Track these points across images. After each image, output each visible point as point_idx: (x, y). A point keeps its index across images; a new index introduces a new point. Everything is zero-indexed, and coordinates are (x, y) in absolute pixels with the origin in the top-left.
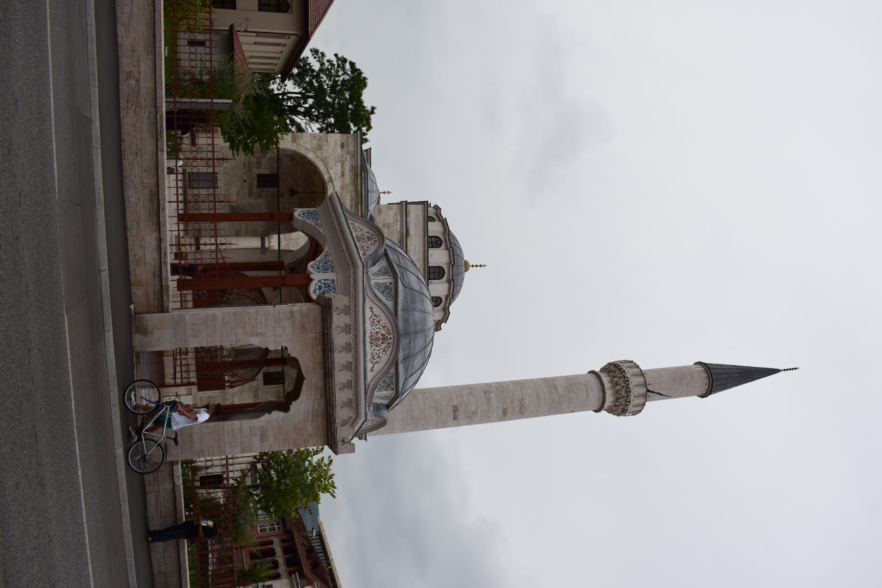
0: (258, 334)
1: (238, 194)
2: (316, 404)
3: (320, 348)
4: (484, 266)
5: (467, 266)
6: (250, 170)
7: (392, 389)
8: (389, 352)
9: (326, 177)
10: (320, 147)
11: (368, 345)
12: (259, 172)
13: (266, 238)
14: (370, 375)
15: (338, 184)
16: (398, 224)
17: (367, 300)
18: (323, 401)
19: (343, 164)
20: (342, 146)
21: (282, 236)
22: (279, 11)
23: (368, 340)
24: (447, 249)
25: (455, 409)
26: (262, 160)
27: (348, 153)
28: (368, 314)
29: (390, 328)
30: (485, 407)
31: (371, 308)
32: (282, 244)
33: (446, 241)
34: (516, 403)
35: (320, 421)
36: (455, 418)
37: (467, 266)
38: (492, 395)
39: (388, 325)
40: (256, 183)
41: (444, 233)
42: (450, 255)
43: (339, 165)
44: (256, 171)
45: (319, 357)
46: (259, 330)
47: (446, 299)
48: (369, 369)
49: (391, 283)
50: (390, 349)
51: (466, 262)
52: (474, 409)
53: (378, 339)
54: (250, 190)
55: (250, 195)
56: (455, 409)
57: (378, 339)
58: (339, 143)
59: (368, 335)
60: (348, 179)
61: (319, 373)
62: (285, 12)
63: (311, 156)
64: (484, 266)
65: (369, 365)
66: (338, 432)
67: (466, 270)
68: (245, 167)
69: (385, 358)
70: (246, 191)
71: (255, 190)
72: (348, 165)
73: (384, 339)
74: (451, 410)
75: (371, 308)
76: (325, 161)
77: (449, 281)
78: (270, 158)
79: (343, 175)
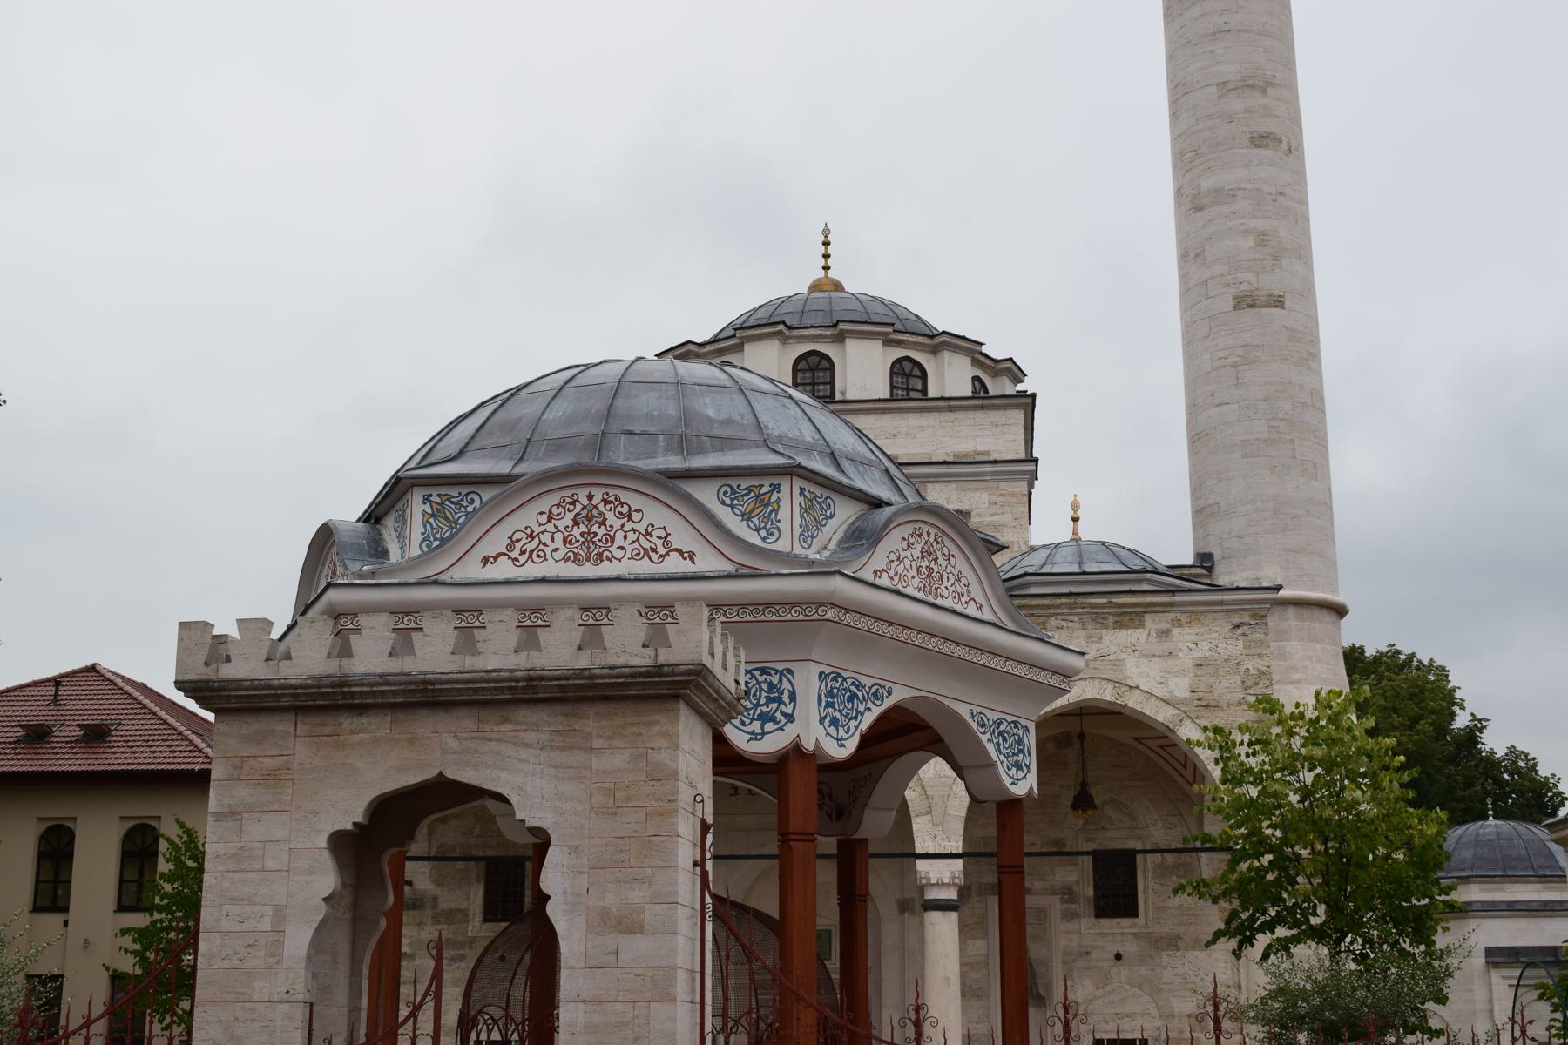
0: (278, 930)
2: (531, 737)
3: (347, 722)
5: (827, 286)
7: (776, 488)
8: (635, 501)
11: (606, 569)
12: (479, 917)
14: (708, 562)
17: (457, 574)
18: (526, 715)
22: (71, 855)
23: (588, 570)
25: (1246, 302)
26: (444, 905)
28: (503, 569)
29: (555, 498)
30: (1243, 205)
31: (486, 560)
34: (1236, 104)
35: (592, 723)
36: (1278, 303)
37: (827, 286)
38: (1207, 183)
39: (546, 504)
42: (760, 338)
45: (376, 726)
46: (266, 925)
47: (899, 344)
48: (687, 567)
49: (427, 499)
50: (625, 496)
51: (815, 287)
52: (1250, 242)
53: (589, 536)
56: (1246, 302)
57: (589, 536)
59: (571, 570)
61: (427, 726)
62: (71, 835)
65: (674, 564)
66: (621, 661)
67: (838, 286)
69: (654, 514)
73: (589, 518)
74: (1248, 317)
75: (486, 560)
77: (840, 338)
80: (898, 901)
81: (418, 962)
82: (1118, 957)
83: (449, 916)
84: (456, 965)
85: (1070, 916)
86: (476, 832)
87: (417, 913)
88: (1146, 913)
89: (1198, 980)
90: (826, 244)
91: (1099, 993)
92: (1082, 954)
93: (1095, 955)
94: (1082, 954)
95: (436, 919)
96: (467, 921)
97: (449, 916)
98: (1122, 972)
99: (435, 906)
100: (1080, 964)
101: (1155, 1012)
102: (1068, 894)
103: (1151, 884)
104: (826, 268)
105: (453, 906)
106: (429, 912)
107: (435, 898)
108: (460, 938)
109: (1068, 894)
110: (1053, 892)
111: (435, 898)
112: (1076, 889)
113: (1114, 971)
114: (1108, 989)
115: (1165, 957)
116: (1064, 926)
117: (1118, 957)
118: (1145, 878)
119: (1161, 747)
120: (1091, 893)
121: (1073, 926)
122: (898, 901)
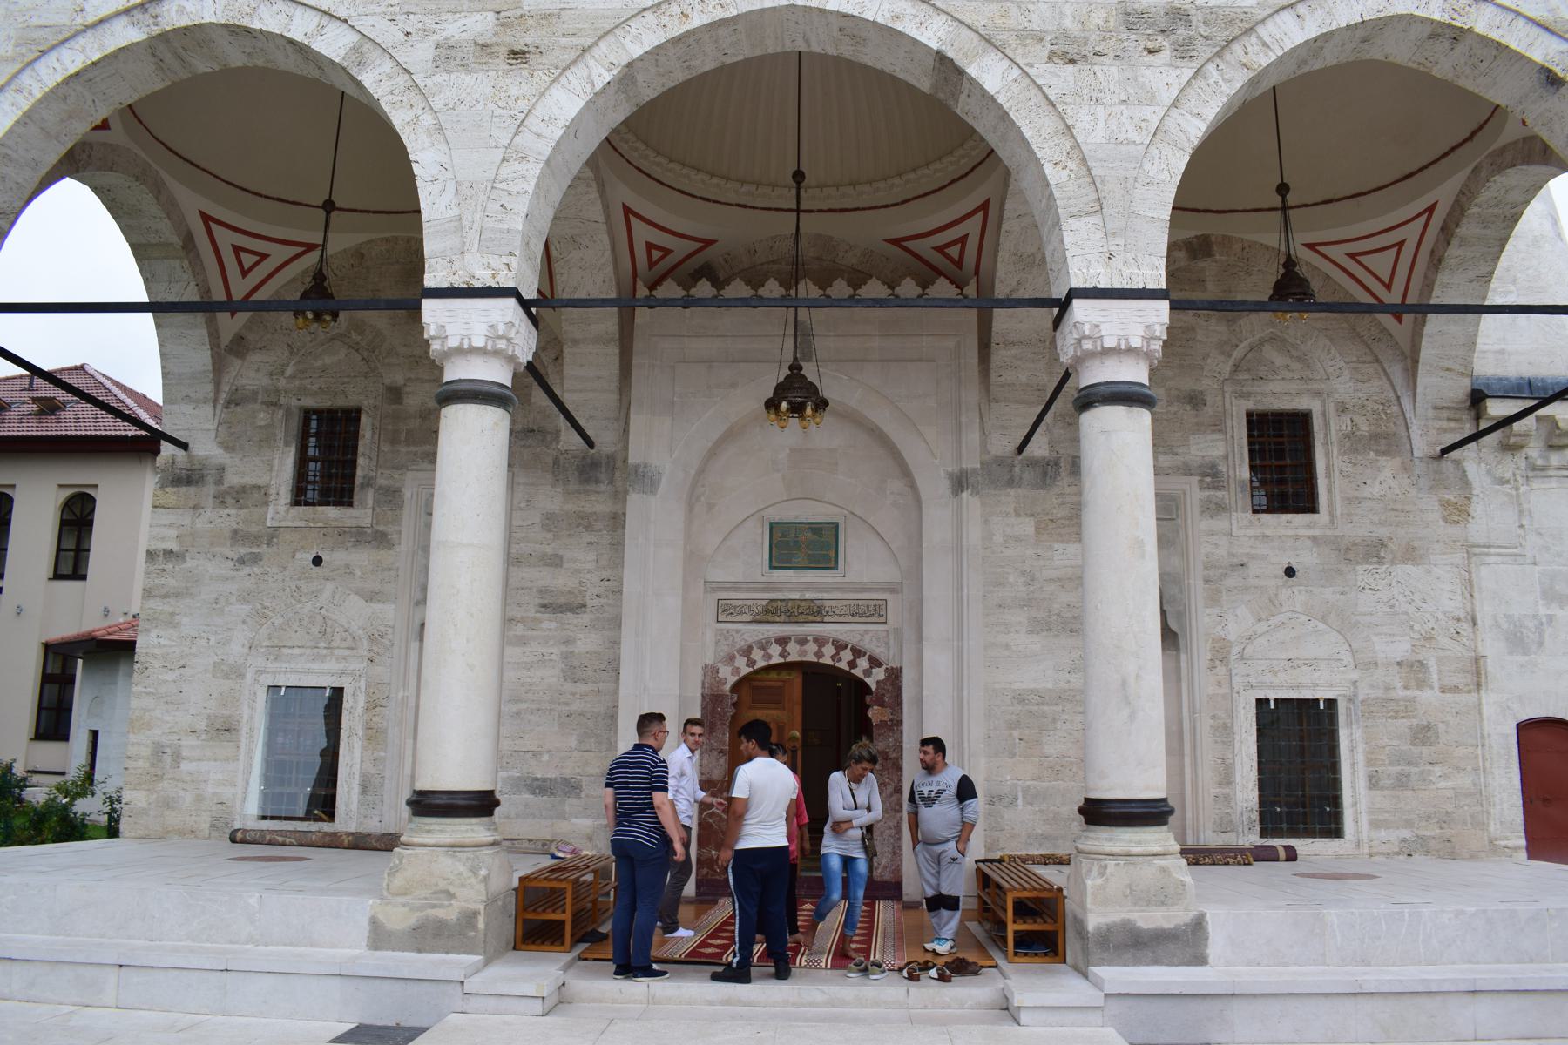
1: (371, 597)
6: (272, 536)
13: (455, 372)
21: (430, 281)
26: (232, 479)
32: (483, 279)
40: (331, 512)
44: (279, 510)
54: (359, 537)
55: (381, 539)
68: (256, 559)
70: (362, 558)
71: (359, 515)
78: (228, 448)
80: (950, 475)
81: (189, 564)
82: (1290, 572)
83: (239, 496)
84: (246, 570)
85: (1216, 509)
86: (289, 372)
87: (192, 490)
88: (1331, 505)
89: (1412, 609)
91: (1262, 627)
92: (1233, 567)
93: (1254, 568)
94: (1233, 567)
95: (220, 501)
96: (266, 504)
97: (239, 496)
98: (1295, 596)
99: (219, 481)
100: (1230, 582)
101: (1347, 658)
102: (1211, 475)
103: (1337, 462)
105: (247, 480)
106: (210, 489)
107: (221, 469)
108: (254, 529)
109: (1211, 475)
110: (1187, 471)
111: (221, 469)
112: (1222, 468)
113: (1284, 594)
114: (1274, 621)
115: (1363, 574)
116: (1205, 524)
117: (1290, 572)
118: (1327, 454)
119: (1353, 256)
120: (1246, 473)
121: (1219, 524)
122: (950, 475)
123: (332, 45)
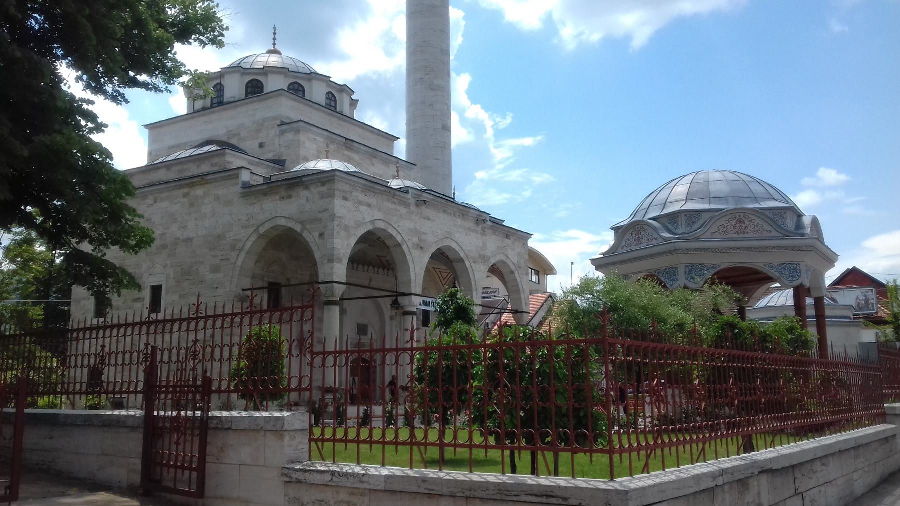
4: (275, 29)
9: (370, 227)
10: (347, 228)
15: (378, 215)
16: (318, 138)
19: (360, 203)
20: (345, 199)
24: (310, 80)
27: (351, 192)
33: (297, 77)
41: (286, 76)
43: (363, 208)
58: (343, 202)
60: (372, 200)
63: (353, 241)
64: (275, 29)
72: (362, 197)
76: (359, 225)
79: (370, 206)
90: (275, 34)
104: (274, 44)
123: (399, 239)
